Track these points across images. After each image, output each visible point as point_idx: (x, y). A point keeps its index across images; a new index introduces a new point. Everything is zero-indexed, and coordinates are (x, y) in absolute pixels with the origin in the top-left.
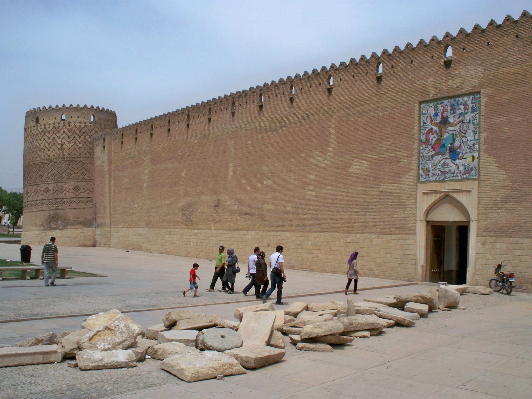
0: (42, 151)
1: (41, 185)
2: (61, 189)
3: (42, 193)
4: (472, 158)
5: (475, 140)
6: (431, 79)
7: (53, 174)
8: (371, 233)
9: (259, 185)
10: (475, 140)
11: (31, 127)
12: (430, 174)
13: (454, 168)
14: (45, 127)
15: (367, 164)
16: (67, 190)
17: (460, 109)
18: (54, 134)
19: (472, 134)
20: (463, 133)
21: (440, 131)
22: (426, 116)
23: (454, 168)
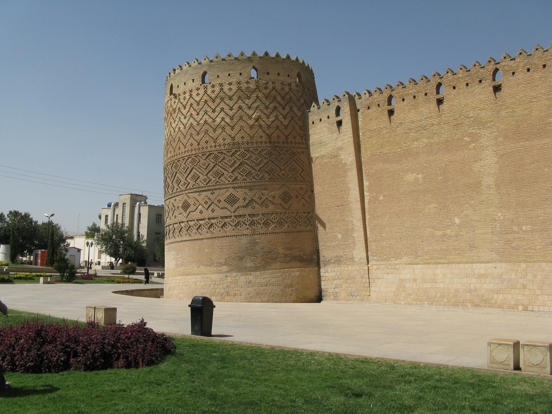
0: (219, 131)
1: (218, 191)
2: (260, 198)
3: (223, 204)
7: (244, 171)
11: (191, 91)
14: (222, 90)
16: (270, 199)
18: (240, 101)
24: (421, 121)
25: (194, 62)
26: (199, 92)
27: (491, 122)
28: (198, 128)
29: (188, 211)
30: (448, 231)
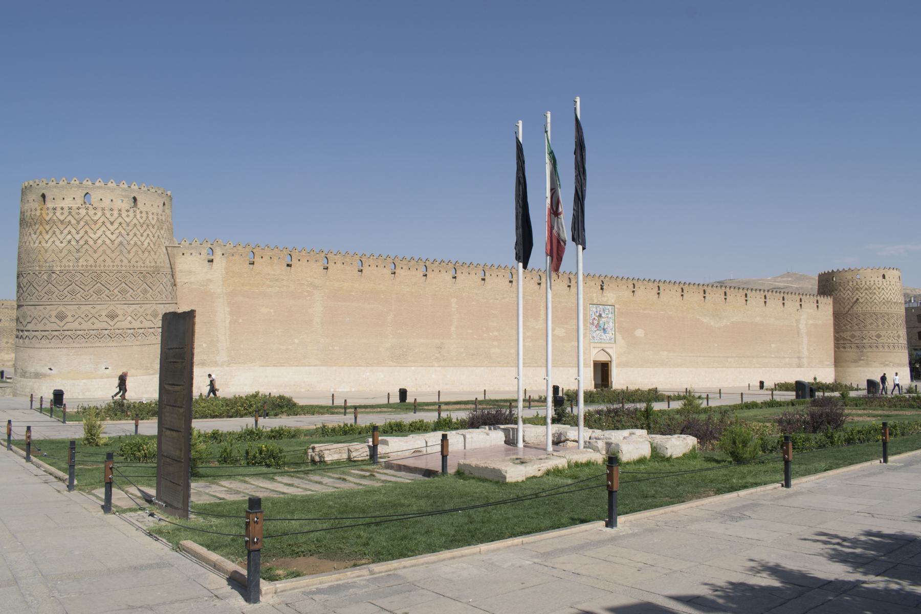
0: (146, 254)
3: (148, 317)
6: (595, 295)
9: (485, 335)
15: (564, 331)
23: (605, 337)
24: (275, 275)
25: (123, 184)
26: (129, 213)
27: (321, 287)
28: (129, 248)
29: (116, 320)
30: (290, 347)
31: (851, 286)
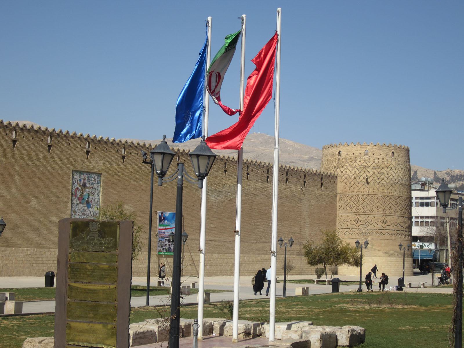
4: (97, 208)
5: (98, 199)
8: (43, 248)
10: (98, 199)
12: (77, 214)
13: (89, 212)
15: (41, 202)
17: (92, 180)
19: (97, 195)
20: (93, 194)
21: (82, 190)
22: (75, 179)
31: (359, 163)
